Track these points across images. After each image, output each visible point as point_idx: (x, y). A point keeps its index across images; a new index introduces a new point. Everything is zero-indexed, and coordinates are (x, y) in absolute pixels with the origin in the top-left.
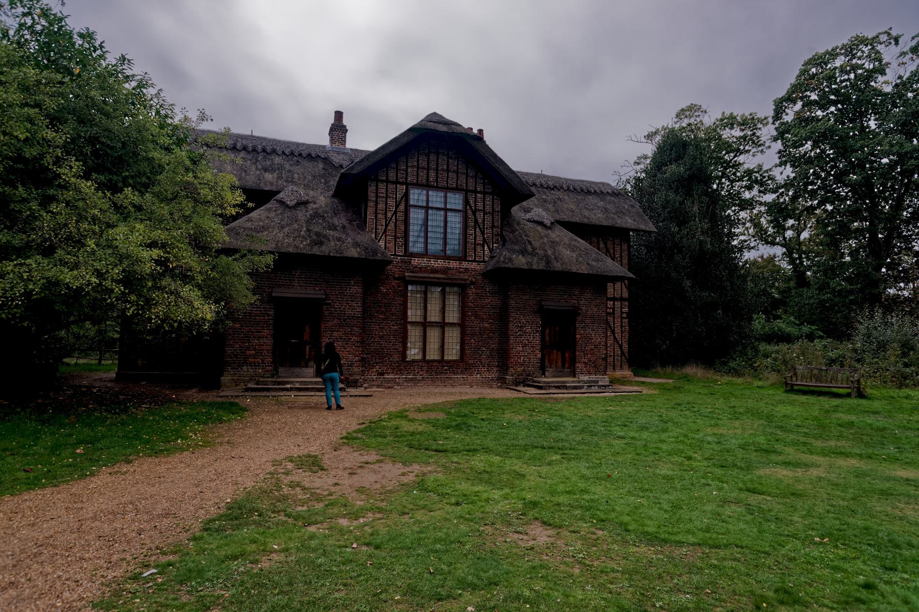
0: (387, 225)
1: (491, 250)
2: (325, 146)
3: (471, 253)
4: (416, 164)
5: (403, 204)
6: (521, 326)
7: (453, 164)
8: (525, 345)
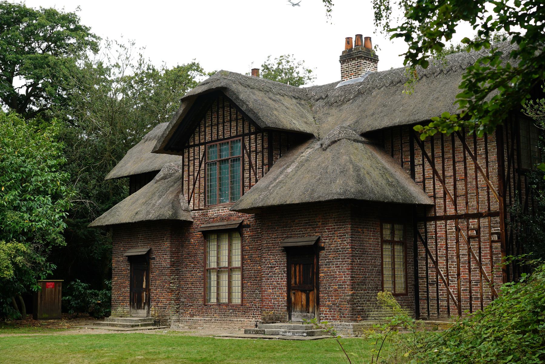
2: (333, 85)
6: (272, 267)
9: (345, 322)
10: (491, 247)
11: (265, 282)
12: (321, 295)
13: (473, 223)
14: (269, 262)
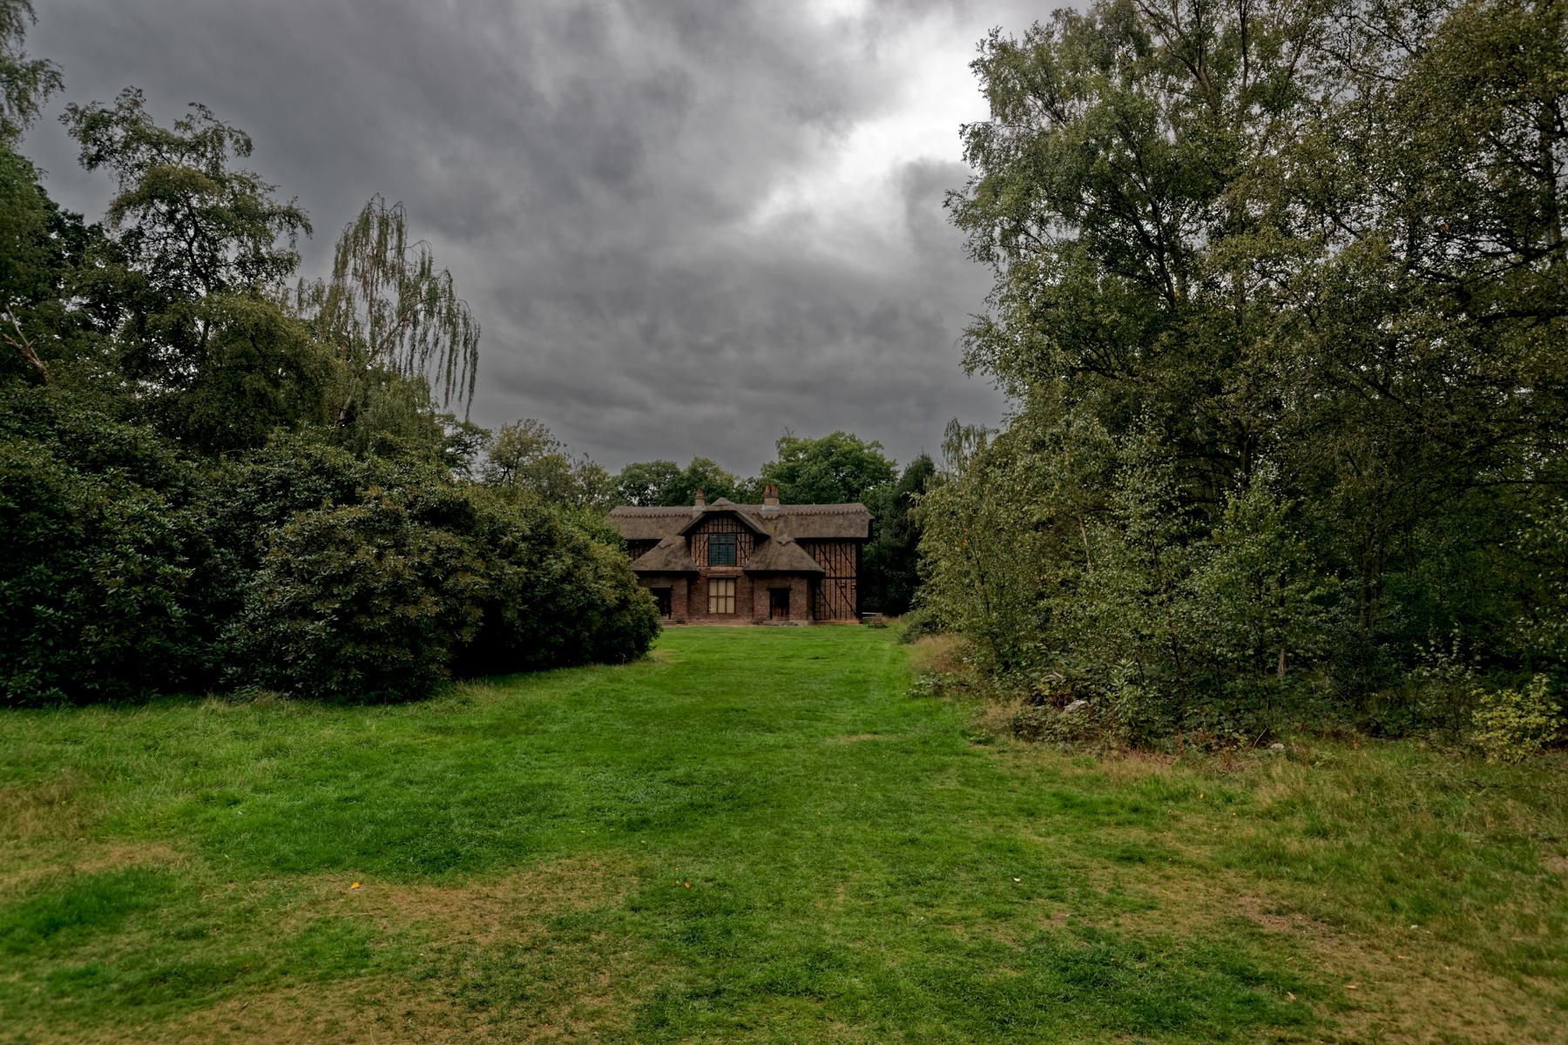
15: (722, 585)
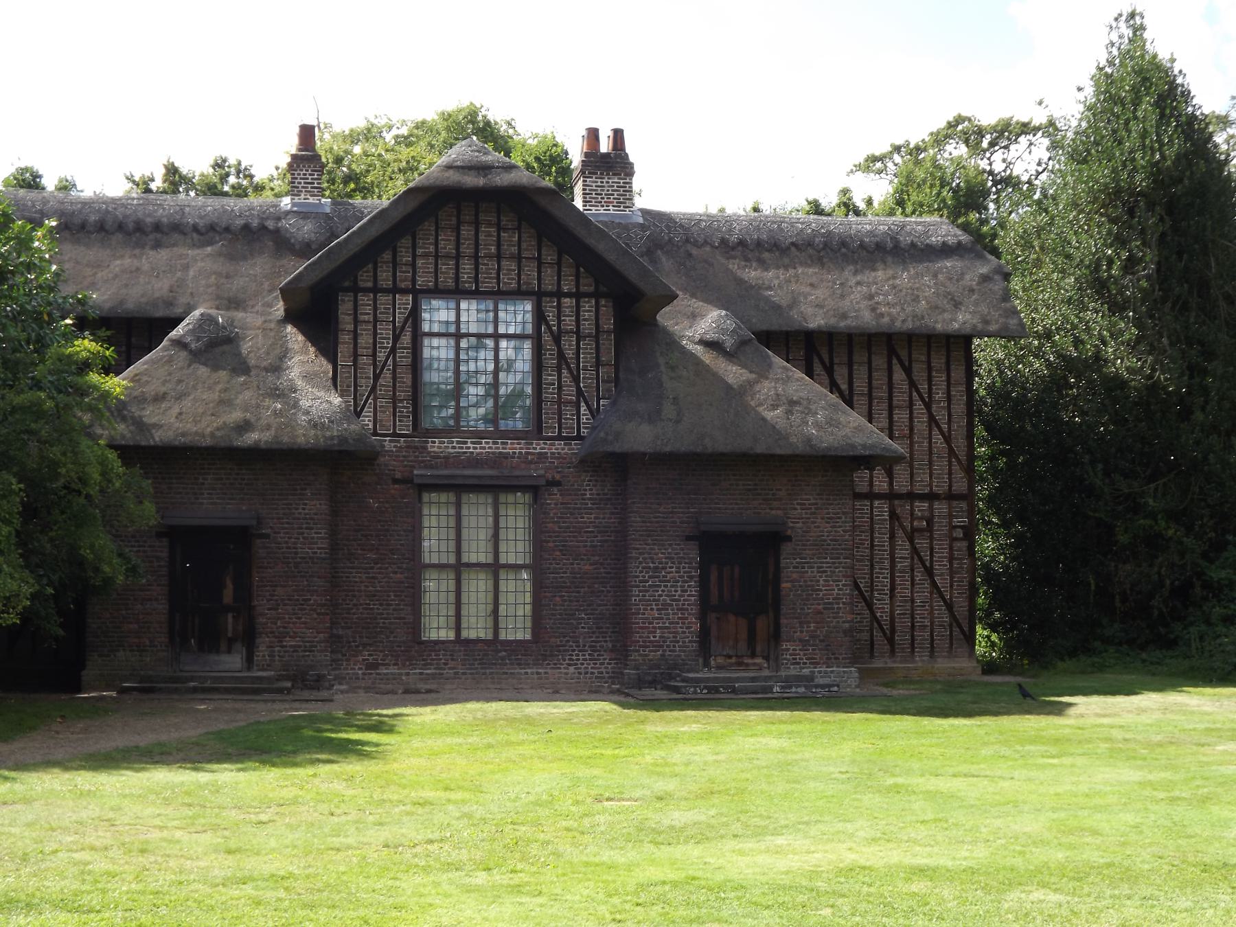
0: (376, 377)
1: (594, 413)
3: (550, 422)
4: (432, 248)
5: (408, 329)
6: (657, 568)
7: (510, 240)
8: (665, 606)
9: (838, 667)
10: (951, 548)
11: (638, 596)
12: (783, 621)
13: (921, 507)
14: (652, 558)
15: (477, 512)
